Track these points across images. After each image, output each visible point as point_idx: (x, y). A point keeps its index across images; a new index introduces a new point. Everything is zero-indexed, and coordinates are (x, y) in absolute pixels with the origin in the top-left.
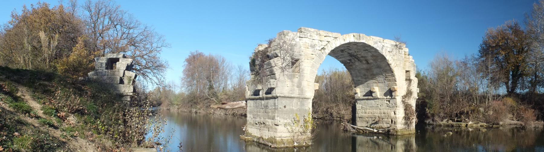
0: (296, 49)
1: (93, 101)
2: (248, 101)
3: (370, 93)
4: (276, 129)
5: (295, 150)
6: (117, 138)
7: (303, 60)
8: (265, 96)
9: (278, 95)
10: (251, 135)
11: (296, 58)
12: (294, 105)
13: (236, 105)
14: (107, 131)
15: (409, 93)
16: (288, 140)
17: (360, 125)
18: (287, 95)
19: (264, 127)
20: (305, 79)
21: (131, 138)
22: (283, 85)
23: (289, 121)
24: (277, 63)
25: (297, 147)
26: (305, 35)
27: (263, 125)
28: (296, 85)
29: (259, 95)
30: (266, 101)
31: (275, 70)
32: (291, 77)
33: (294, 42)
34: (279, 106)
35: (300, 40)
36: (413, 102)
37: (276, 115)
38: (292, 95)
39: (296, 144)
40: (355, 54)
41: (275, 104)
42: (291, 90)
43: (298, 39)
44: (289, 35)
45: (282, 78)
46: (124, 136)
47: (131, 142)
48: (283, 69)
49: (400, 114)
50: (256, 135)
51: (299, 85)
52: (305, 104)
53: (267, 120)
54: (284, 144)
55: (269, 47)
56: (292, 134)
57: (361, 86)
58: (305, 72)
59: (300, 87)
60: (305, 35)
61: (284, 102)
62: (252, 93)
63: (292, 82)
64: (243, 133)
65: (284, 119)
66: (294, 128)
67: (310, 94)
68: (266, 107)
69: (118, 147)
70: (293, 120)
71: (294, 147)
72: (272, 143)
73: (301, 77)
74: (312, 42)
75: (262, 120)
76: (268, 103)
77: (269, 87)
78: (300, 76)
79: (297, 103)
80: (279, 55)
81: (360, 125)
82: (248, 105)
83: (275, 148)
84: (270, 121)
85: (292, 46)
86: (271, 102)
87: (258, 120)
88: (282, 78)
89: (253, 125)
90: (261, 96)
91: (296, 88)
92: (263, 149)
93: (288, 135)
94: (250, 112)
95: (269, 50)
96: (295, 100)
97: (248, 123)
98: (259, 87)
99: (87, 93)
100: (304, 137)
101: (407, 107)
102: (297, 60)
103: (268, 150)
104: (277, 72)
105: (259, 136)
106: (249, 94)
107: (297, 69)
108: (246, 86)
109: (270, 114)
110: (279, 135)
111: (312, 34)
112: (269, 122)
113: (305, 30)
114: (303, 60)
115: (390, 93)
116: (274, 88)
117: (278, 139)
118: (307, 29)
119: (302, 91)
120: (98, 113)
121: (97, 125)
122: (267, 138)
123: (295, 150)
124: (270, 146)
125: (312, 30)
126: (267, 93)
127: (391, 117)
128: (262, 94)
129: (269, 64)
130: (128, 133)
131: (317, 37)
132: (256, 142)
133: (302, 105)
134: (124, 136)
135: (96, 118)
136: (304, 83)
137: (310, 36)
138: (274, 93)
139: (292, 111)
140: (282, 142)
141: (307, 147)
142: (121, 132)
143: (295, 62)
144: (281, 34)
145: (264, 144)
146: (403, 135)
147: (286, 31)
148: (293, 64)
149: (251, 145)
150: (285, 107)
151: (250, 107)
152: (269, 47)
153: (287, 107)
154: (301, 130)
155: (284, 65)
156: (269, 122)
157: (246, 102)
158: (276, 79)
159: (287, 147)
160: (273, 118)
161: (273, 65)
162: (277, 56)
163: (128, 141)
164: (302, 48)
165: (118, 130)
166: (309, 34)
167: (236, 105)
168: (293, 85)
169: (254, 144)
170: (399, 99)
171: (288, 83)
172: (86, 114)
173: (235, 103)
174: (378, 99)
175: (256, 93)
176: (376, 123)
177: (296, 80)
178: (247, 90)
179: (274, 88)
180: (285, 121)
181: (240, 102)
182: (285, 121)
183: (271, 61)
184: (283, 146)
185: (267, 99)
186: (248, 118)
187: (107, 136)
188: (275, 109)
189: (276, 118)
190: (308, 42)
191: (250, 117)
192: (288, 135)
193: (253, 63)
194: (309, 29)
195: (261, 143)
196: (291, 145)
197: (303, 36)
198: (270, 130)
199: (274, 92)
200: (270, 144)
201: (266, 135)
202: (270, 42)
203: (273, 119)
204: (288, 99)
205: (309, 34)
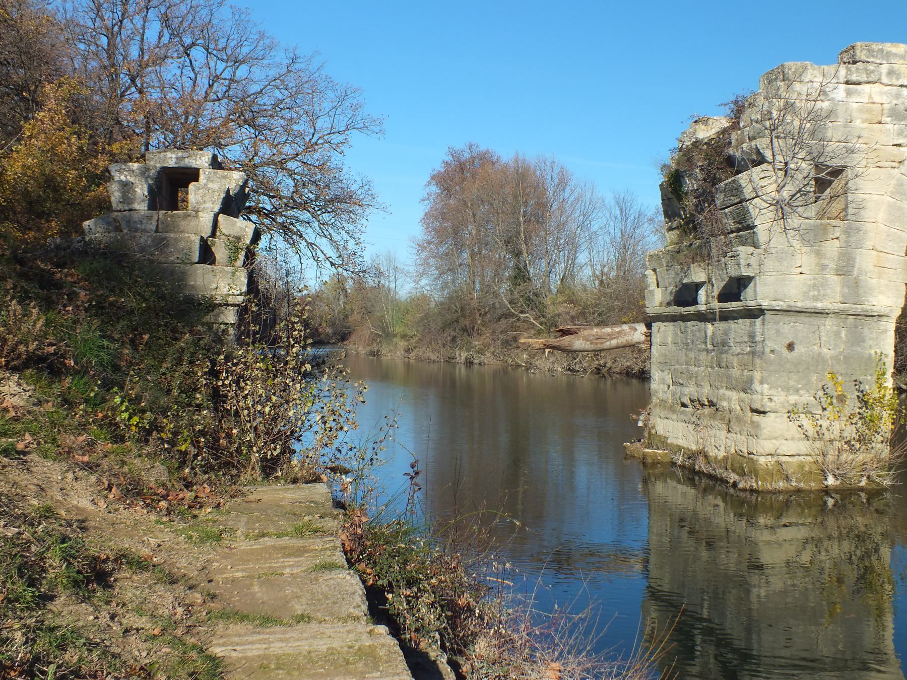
0: (833, 131)
1: (96, 322)
2: (655, 326)
4: (756, 426)
5: (830, 502)
6: (186, 453)
7: (859, 170)
8: (716, 305)
9: (765, 304)
10: (663, 442)
11: (836, 163)
12: (827, 342)
13: (611, 337)
14: (149, 432)
16: (801, 466)
18: (800, 305)
19: (712, 417)
20: (869, 244)
21: (239, 451)
23: (806, 398)
24: (762, 184)
25: (837, 490)
26: (869, 73)
27: (707, 410)
28: (832, 265)
29: (695, 302)
30: (721, 325)
31: (753, 212)
32: (814, 238)
33: (826, 105)
34: (770, 345)
35: (849, 93)
37: (757, 375)
38: (819, 305)
39: (831, 481)
41: (752, 336)
43: (840, 92)
44: (807, 77)
45: (778, 242)
46: (214, 447)
47: (241, 467)
48: (782, 208)
50: (681, 442)
51: (845, 268)
53: (723, 391)
54: (787, 479)
55: (735, 126)
56: (818, 444)
58: (867, 215)
60: (869, 73)
61: (789, 329)
62: (669, 298)
63: (818, 254)
64: (638, 434)
65: (787, 389)
66: (825, 423)
68: (721, 345)
69: (188, 485)
70: (821, 393)
71: (827, 491)
72: (742, 474)
74: (898, 96)
75: (706, 392)
76: (726, 333)
77: (734, 273)
78: (847, 232)
79: (837, 334)
80: (768, 155)
82: (657, 339)
83: (752, 491)
84: (734, 395)
85: (818, 119)
86: (740, 327)
87: (691, 390)
88: (778, 242)
89: (672, 409)
90: (702, 307)
92: (706, 491)
93: (803, 447)
94: (664, 364)
95: (734, 136)
96: (829, 324)
97: (654, 400)
98: (698, 274)
99: (73, 296)
100: (860, 457)
102: (837, 172)
103: (724, 496)
104: (762, 218)
105: (694, 447)
106: (657, 298)
107: (837, 206)
108: (649, 272)
109: (736, 372)
110: (767, 446)
112: (729, 400)
113: (870, 51)
114: (859, 170)
116: (750, 279)
117: (762, 460)
118: (876, 47)
119: (855, 287)
120: (116, 368)
121: (114, 409)
122: (721, 454)
123: (830, 502)
124: (735, 485)
126: (725, 296)
128: (705, 300)
129: (736, 189)
130: (229, 436)
132: (683, 467)
133: (857, 339)
134: (214, 447)
135: (107, 385)
136: (865, 260)
137: (891, 73)
139: (819, 360)
140: (780, 471)
141: (875, 493)
142: (202, 433)
143: (827, 178)
144: (778, 76)
145: (710, 477)
147: (791, 66)
148: (822, 185)
149: (663, 476)
150: (791, 347)
151: (663, 344)
152: (735, 126)
153: (799, 349)
154: (850, 432)
155: (786, 194)
156: (731, 400)
157: (649, 326)
158: (756, 246)
159: (798, 491)
160: (746, 387)
161: (748, 192)
162: (760, 160)
163: (228, 464)
164: (858, 123)
165: (191, 424)
166: (884, 68)
167: (611, 337)
168: (823, 267)
169: (673, 476)
171: (805, 258)
172: (69, 371)
173: (608, 330)
175: (686, 295)
177: (832, 248)
178: (653, 286)
179: (750, 279)
180: (793, 399)
181: (625, 327)
182: (793, 399)
183: (743, 178)
184: (781, 485)
185: (726, 316)
186: (654, 386)
187: (148, 449)
188: (753, 353)
189: (757, 386)
190: (877, 99)
191: (663, 381)
192: (803, 447)
193: (673, 188)
194: (888, 47)
195: (700, 473)
196: (813, 485)
197: (864, 78)
198: (735, 427)
199: (749, 292)
200: (733, 477)
201: (719, 443)
202: (739, 109)
203: (745, 391)
204: (803, 318)
205: (884, 68)
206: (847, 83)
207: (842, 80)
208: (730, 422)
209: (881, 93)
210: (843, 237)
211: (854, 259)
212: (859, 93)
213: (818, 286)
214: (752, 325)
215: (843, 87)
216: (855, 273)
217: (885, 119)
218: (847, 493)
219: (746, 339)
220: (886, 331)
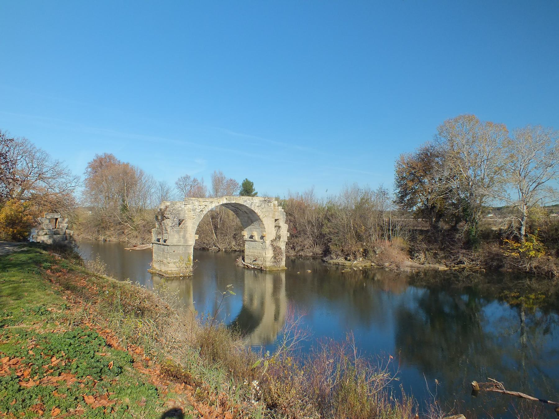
3: (251, 237)
10: (155, 269)
12: (181, 250)
15: (278, 237)
17: (247, 261)
22: (173, 238)
24: (168, 223)
32: (178, 232)
36: (282, 245)
43: (183, 206)
45: (172, 233)
49: (270, 254)
51: (184, 237)
57: (247, 229)
58: (188, 228)
61: (174, 248)
65: (173, 259)
67: (192, 243)
68: (164, 251)
73: (186, 231)
75: (161, 259)
81: (247, 261)
82: (154, 247)
93: (177, 269)
98: (160, 237)
101: (276, 250)
104: (169, 230)
110: (170, 269)
111: (193, 201)
115: (262, 237)
119: (186, 241)
125: (194, 199)
128: (161, 242)
129: (164, 223)
131: (197, 203)
136: (188, 236)
138: (168, 243)
140: (172, 273)
141: (189, 277)
146: (271, 272)
148: (180, 224)
149: (155, 275)
156: (165, 261)
170: (268, 242)
171: (177, 236)
174: (256, 241)
176: (255, 261)
177: (182, 233)
192: (177, 269)
201: (164, 269)
208: (164, 264)
213: (179, 241)
218: (184, 277)
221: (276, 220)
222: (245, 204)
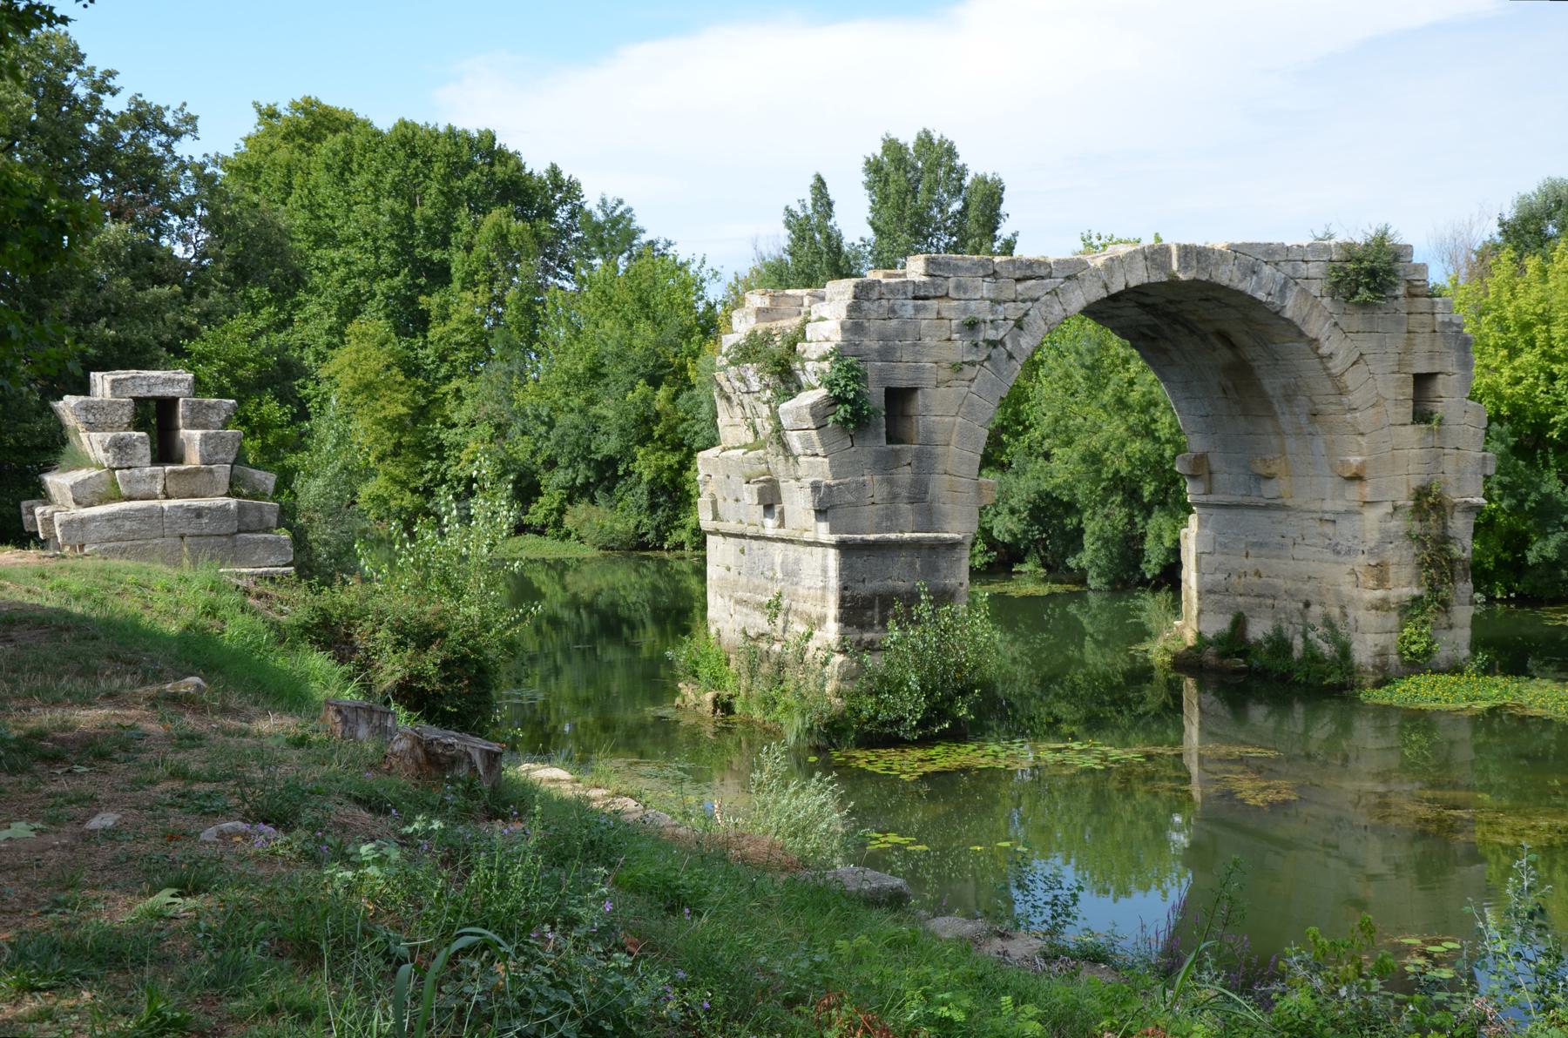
20: (940, 468)
28: (905, 493)
35: (917, 309)
40: (1172, 309)
42: (888, 517)
51: (919, 496)
52: (943, 564)
59: (922, 500)
63: (891, 482)
74: (965, 310)
76: (797, 561)
91: (904, 507)
111: (966, 279)
127: (1338, 594)
136: (939, 485)
137: (958, 287)
166: (952, 282)
177: (904, 475)
186: (711, 613)
190: (944, 314)
205: (952, 282)
206: (915, 298)
207: (910, 295)
209: (950, 308)
210: (914, 463)
211: (927, 486)
212: (925, 308)
214: (825, 557)
215: (911, 303)
216: (929, 498)
217: (955, 336)
219: (818, 572)
220: (959, 560)
221: (1423, 381)
222: (1248, 286)
